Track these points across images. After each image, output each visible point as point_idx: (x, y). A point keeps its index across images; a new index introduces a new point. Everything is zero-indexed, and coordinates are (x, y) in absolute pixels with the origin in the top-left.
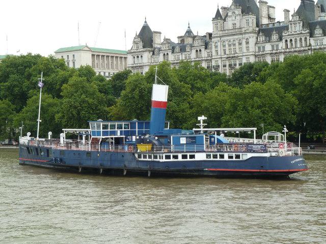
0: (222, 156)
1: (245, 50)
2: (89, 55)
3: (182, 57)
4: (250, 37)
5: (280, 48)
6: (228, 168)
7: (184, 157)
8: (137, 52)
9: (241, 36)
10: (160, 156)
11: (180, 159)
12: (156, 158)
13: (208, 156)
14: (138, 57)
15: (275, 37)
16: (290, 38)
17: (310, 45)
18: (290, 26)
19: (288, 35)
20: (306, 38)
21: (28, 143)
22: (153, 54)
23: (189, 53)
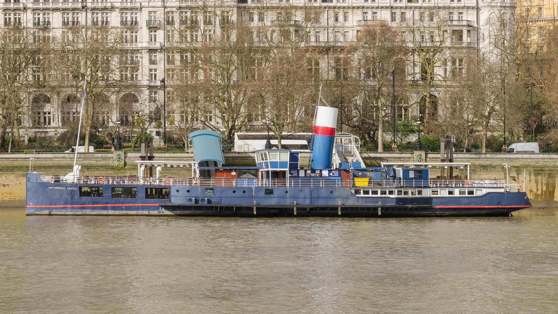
6: (460, 205)
12: (385, 193)
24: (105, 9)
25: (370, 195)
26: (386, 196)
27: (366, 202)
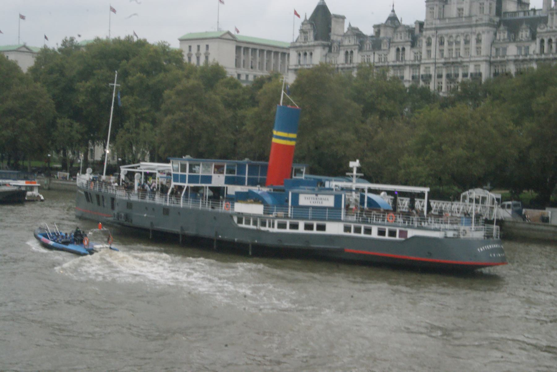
0: (368, 231)
1: (473, 52)
2: (231, 48)
3: (374, 58)
4: (483, 32)
5: (531, 52)
7: (309, 227)
8: (305, 46)
9: (468, 30)
10: (270, 223)
11: (301, 230)
13: (347, 229)
14: (305, 54)
15: (524, 34)
16: (548, 38)
18: (550, 16)
19: (546, 32)
21: (87, 185)
22: (330, 51)
23: (385, 53)
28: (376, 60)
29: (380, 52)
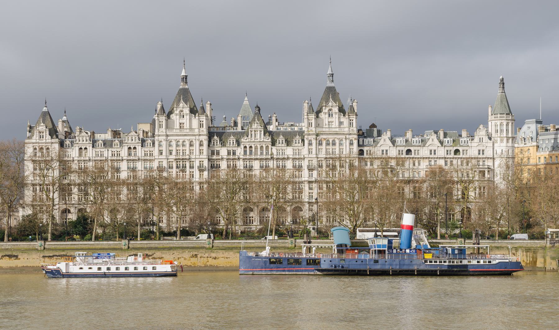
6: (483, 269)
12: (442, 262)
17: (272, 154)
19: (249, 142)
20: (267, 147)
24: (284, 159)
25: (433, 263)
26: (442, 264)
27: (431, 267)
28: (110, 155)
29: (113, 150)
